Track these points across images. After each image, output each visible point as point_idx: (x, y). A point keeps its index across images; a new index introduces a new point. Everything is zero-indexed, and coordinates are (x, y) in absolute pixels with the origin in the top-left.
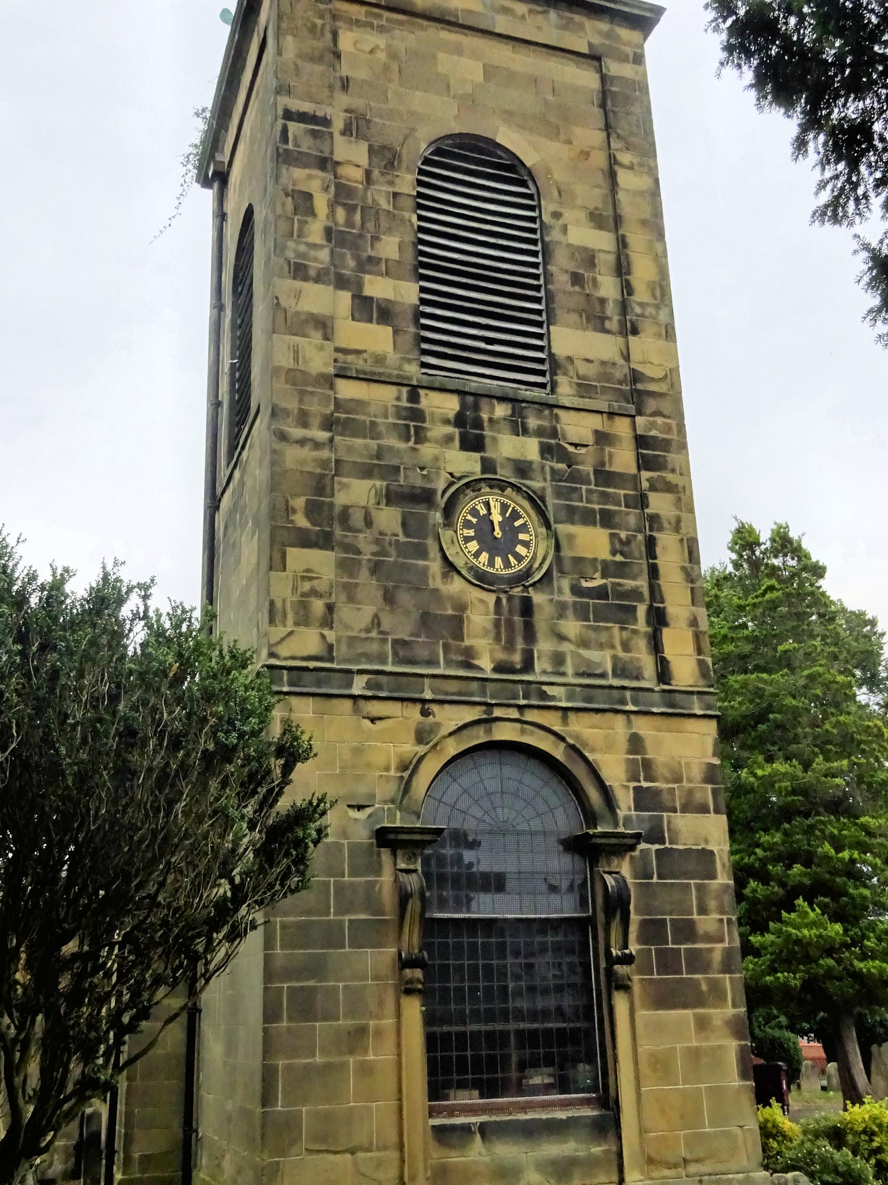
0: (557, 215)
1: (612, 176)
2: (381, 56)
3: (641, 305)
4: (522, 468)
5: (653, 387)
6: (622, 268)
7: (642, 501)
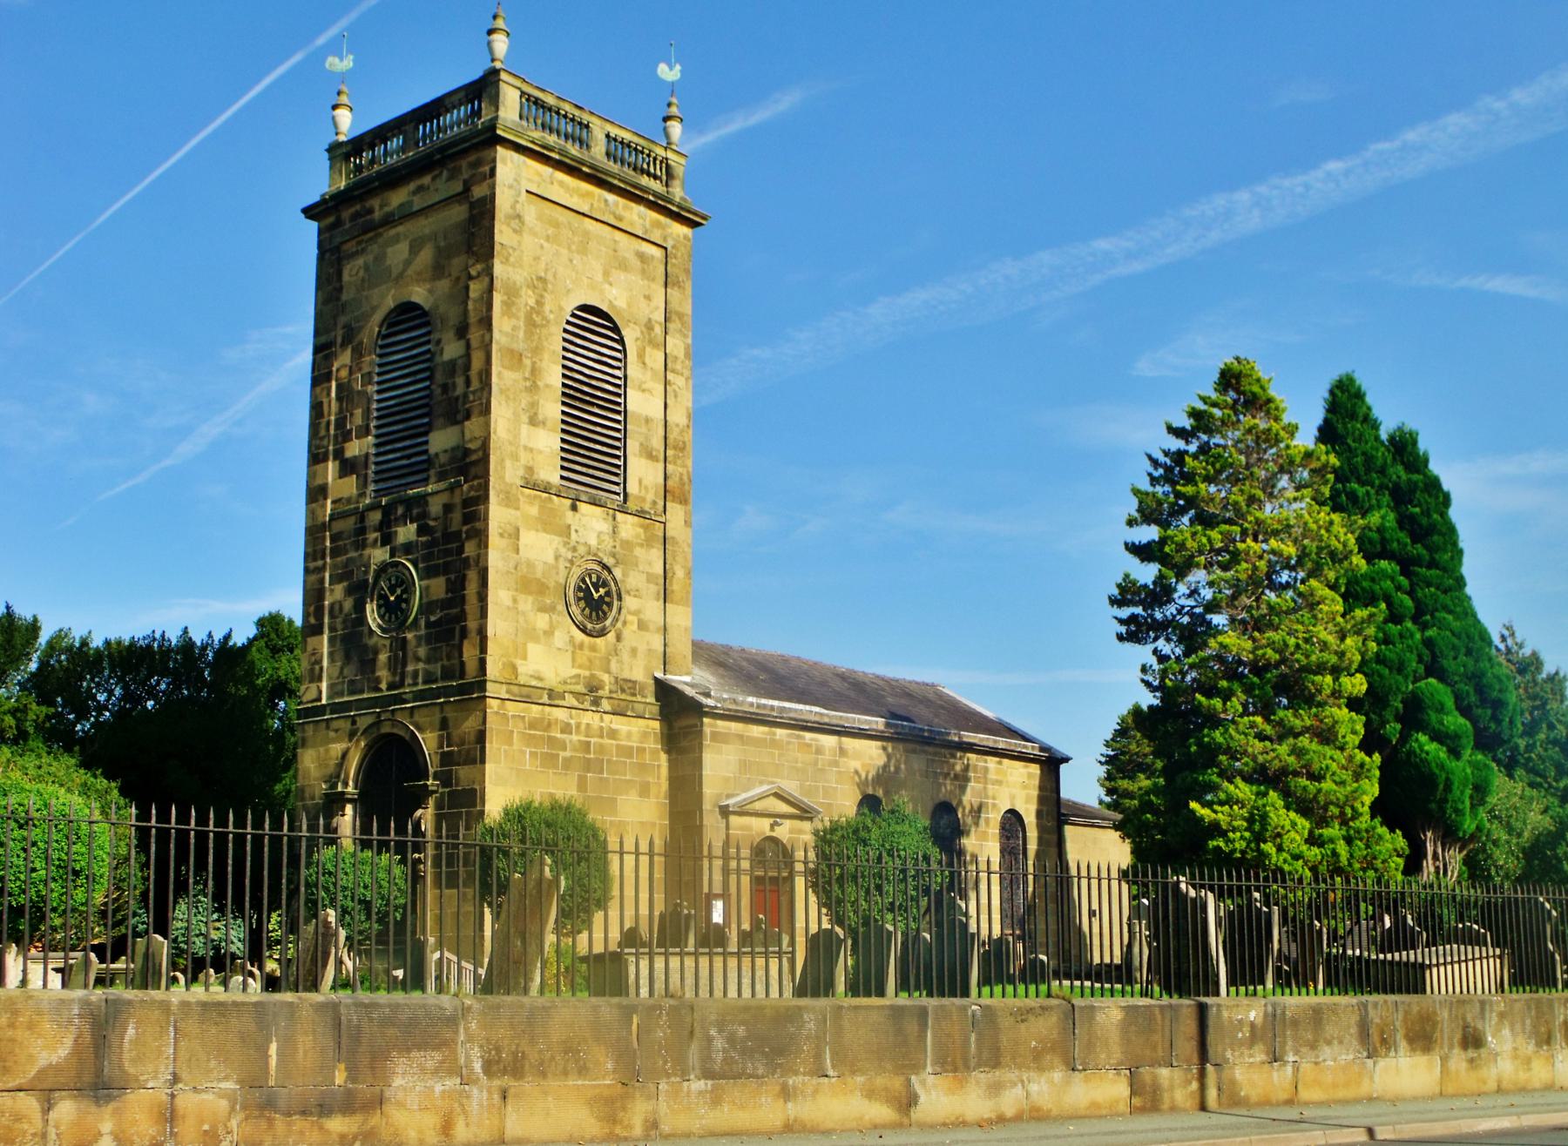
0: (439, 342)
1: (467, 288)
2: (361, 273)
3: (474, 393)
4: (408, 548)
5: (474, 457)
6: (468, 367)
7: (461, 550)
